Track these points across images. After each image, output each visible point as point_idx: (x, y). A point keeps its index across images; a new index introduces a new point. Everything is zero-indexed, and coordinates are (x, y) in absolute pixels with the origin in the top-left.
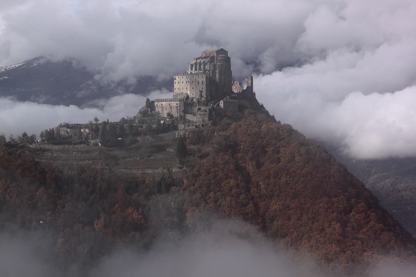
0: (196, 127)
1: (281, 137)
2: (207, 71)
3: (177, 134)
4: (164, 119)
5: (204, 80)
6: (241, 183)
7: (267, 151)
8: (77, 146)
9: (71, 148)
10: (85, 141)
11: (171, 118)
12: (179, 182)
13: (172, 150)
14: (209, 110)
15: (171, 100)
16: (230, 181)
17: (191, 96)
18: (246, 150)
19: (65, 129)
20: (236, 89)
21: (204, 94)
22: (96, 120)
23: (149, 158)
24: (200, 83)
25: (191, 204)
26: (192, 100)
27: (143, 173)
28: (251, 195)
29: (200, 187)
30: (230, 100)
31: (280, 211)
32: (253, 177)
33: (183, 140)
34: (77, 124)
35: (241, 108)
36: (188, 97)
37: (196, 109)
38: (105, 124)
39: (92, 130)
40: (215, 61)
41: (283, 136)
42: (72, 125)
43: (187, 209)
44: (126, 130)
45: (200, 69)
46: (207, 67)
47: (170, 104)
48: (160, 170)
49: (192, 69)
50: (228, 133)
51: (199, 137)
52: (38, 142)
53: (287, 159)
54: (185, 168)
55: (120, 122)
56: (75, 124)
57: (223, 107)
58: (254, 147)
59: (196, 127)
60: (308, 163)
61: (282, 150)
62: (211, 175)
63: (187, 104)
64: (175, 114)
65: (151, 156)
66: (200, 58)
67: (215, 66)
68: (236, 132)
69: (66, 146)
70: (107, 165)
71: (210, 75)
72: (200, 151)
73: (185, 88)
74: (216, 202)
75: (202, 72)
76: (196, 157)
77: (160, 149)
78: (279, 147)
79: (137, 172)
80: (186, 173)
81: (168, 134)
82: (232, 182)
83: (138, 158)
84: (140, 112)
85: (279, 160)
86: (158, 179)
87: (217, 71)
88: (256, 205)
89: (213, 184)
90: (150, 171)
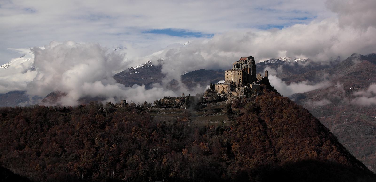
0: (237, 98)
1: (284, 104)
2: (243, 68)
3: (227, 102)
4: (220, 94)
5: (241, 73)
6: (262, 129)
7: (276, 112)
9: (170, 110)
10: (178, 106)
11: (223, 93)
12: (228, 129)
13: (224, 111)
14: (244, 89)
15: (223, 84)
16: (256, 128)
17: (234, 82)
18: (264, 111)
19: (167, 99)
20: (258, 78)
21: (241, 81)
22: (183, 95)
23: (212, 116)
24: (239, 74)
25: (234, 141)
26: (235, 84)
27: (209, 124)
28: (267, 136)
29: (239, 131)
30: (256, 84)
31: (284, 145)
32: (268, 126)
33: (230, 106)
34: (173, 97)
35: (262, 88)
36: (232, 82)
37: (237, 89)
38: (188, 97)
39: (181, 100)
40: (247, 63)
41: (285, 104)
42: (171, 97)
43: (233, 143)
45: (239, 67)
46: (243, 66)
47: (223, 86)
48: (218, 122)
49: (235, 67)
50: (255, 102)
51: (239, 104)
52: (152, 107)
53: (287, 116)
54: (231, 121)
55: (196, 96)
56: (173, 97)
57: (251, 88)
58: (269, 110)
59: (237, 98)
60: (298, 118)
61: (284, 111)
63: (232, 86)
64: (226, 92)
65: (213, 114)
66: (239, 61)
67: (247, 65)
68: (259, 101)
69: (168, 109)
70: (189, 119)
71: (244, 70)
72: (239, 111)
74: (248, 139)
76: (237, 115)
77: (218, 110)
78: (283, 109)
79: (205, 123)
80: (232, 124)
82: (257, 129)
83: (206, 116)
85: (282, 116)
86: (216, 127)
87: (248, 68)
88: (270, 141)
89: (247, 130)
90: (212, 123)
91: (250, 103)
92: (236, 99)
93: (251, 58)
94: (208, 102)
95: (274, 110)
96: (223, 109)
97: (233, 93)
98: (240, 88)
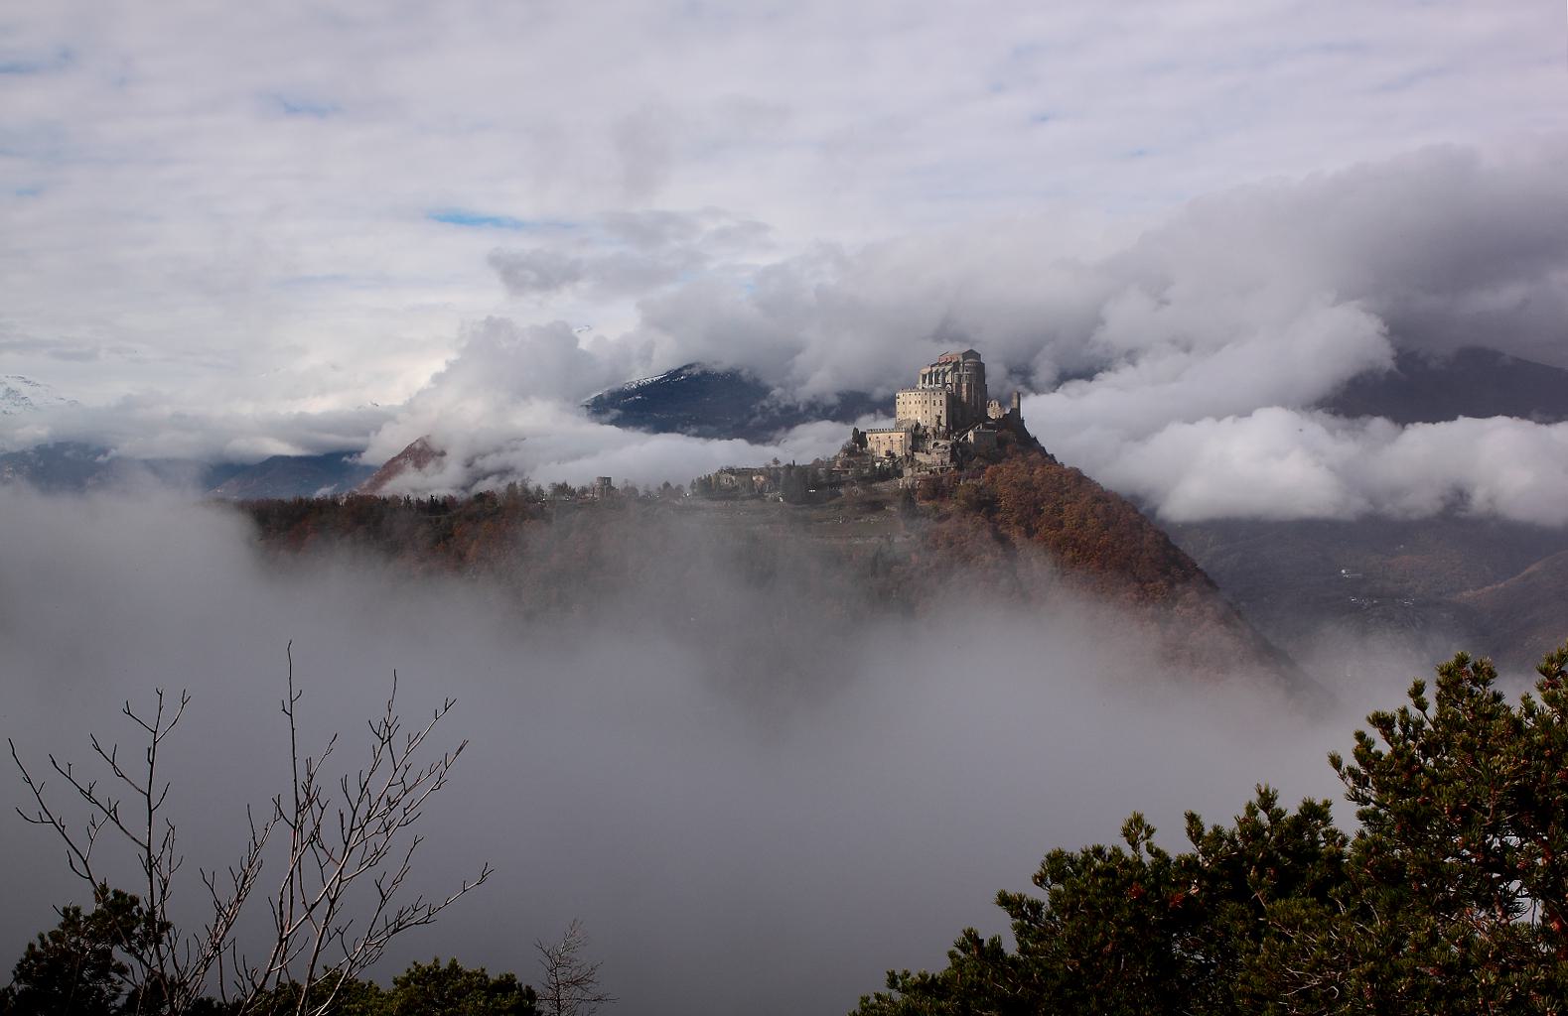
0: (931, 472)
4: (881, 460)
8: (747, 502)
13: (892, 509)
14: (952, 445)
19: (729, 476)
20: (994, 412)
22: (776, 461)
24: (938, 403)
30: (984, 431)
36: (918, 425)
37: (930, 446)
38: (790, 467)
39: (770, 477)
40: (961, 370)
44: (821, 478)
46: (948, 379)
48: (874, 540)
49: (924, 382)
53: (1074, 522)
55: (813, 464)
58: (1022, 504)
62: (954, 546)
63: (917, 437)
64: (899, 453)
65: (860, 518)
67: (960, 376)
73: (913, 412)
75: (940, 386)
77: (876, 506)
81: (886, 483)
84: (844, 450)
85: (1061, 524)
91: (968, 485)
92: (928, 473)
93: (970, 354)
94: (847, 484)
95: (1036, 505)
96: (889, 502)
97: (920, 457)
98: (939, 441)
